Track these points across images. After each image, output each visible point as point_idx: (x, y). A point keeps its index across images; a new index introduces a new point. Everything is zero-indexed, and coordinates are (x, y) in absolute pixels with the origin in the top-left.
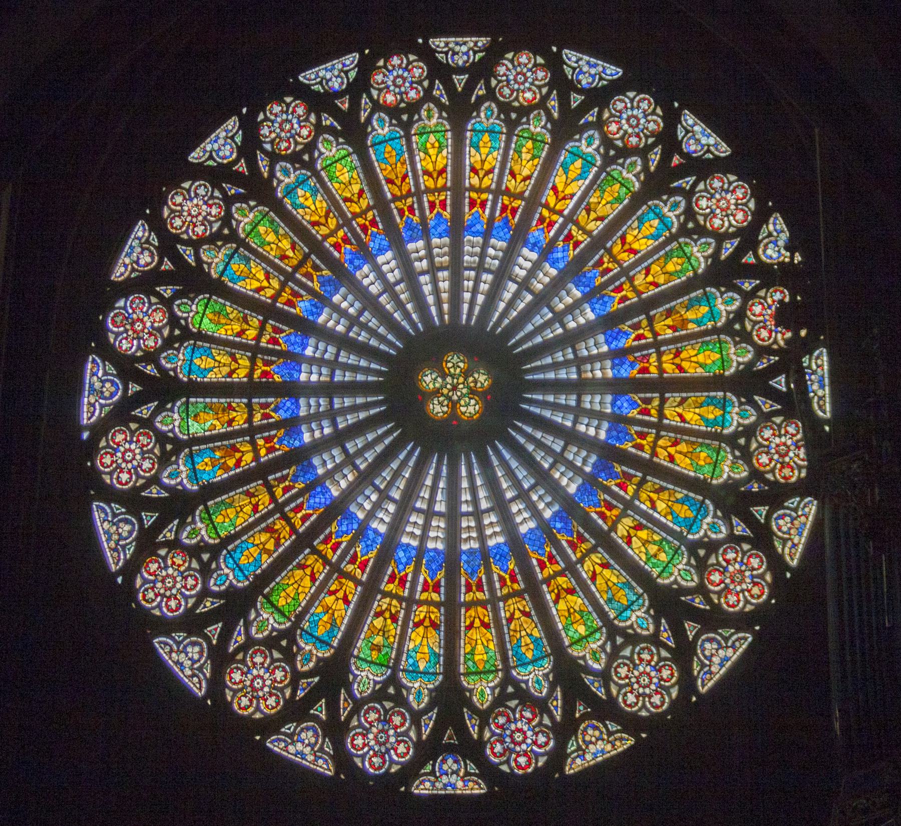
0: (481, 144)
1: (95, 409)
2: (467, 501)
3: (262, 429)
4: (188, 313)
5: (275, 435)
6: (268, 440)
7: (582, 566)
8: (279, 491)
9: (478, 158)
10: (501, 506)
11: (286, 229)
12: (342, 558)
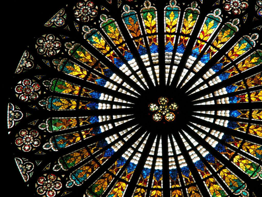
0: (170, 16)
1: (12, 123)
2: (170, 152)
3: (83, 128)
4: (49, 85)
5: (89, 130)
6: (86, 132)
7: (219, 174)
8: (92, 151)
9: (169, 21)
10: (185, 153)
11: (88, 51)
12: (120, 174)
